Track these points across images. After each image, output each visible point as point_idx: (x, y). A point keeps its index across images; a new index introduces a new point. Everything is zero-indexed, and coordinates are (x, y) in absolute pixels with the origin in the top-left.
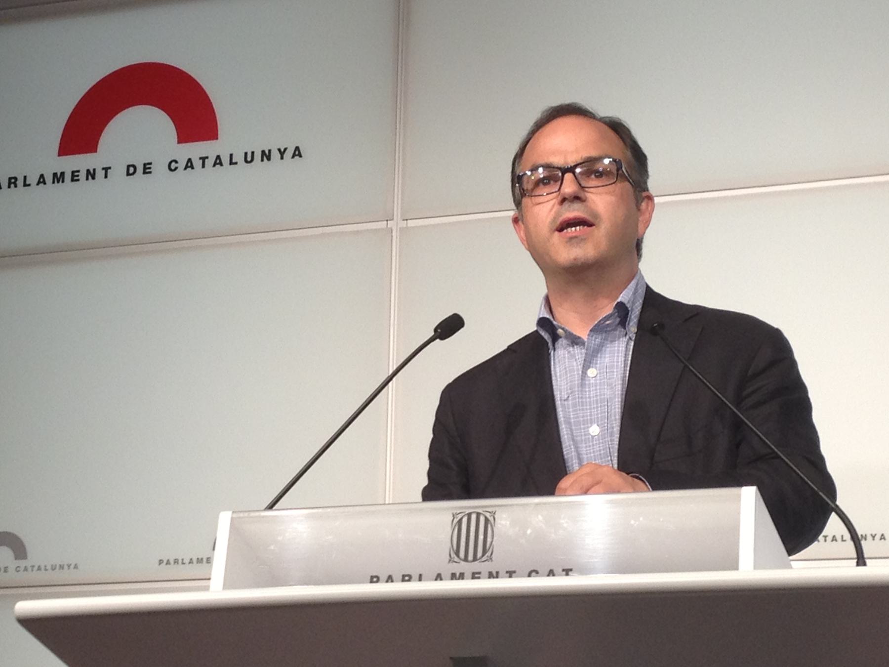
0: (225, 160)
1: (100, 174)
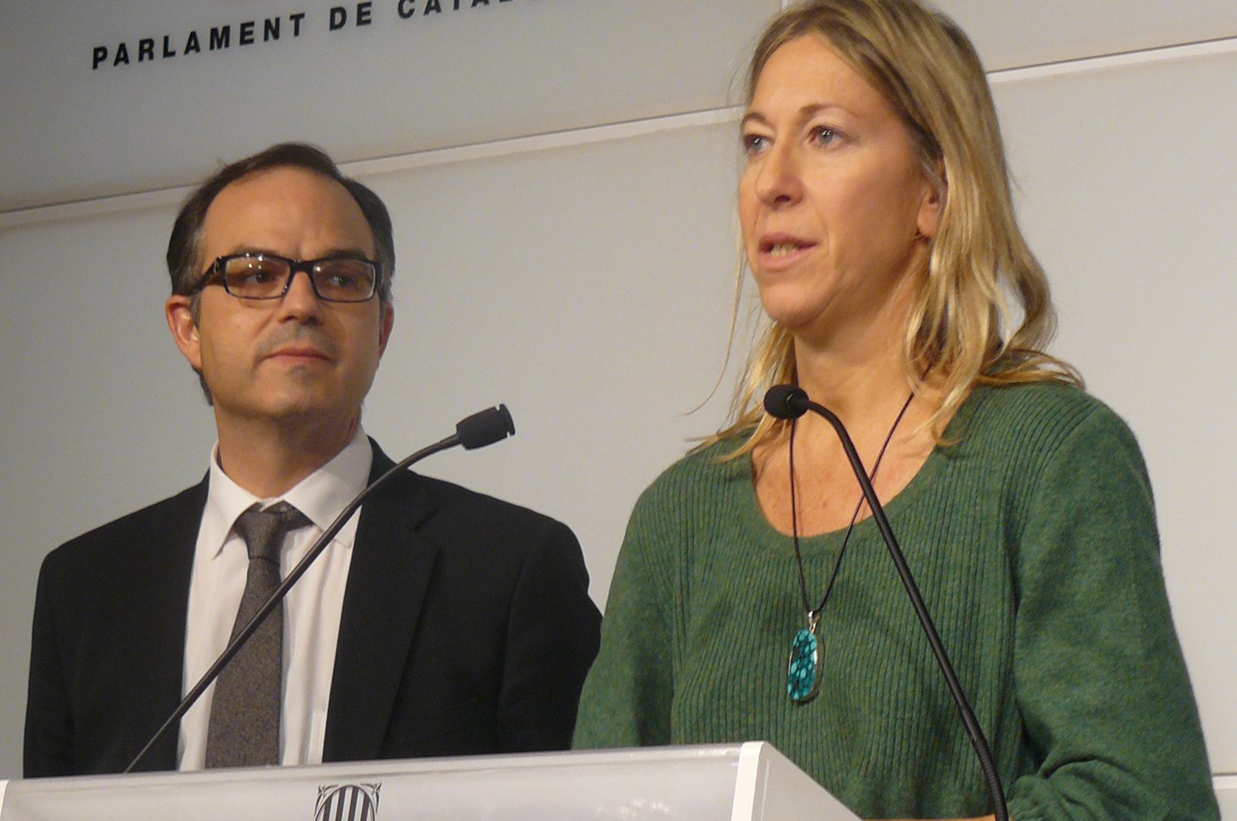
1: (287, 27)
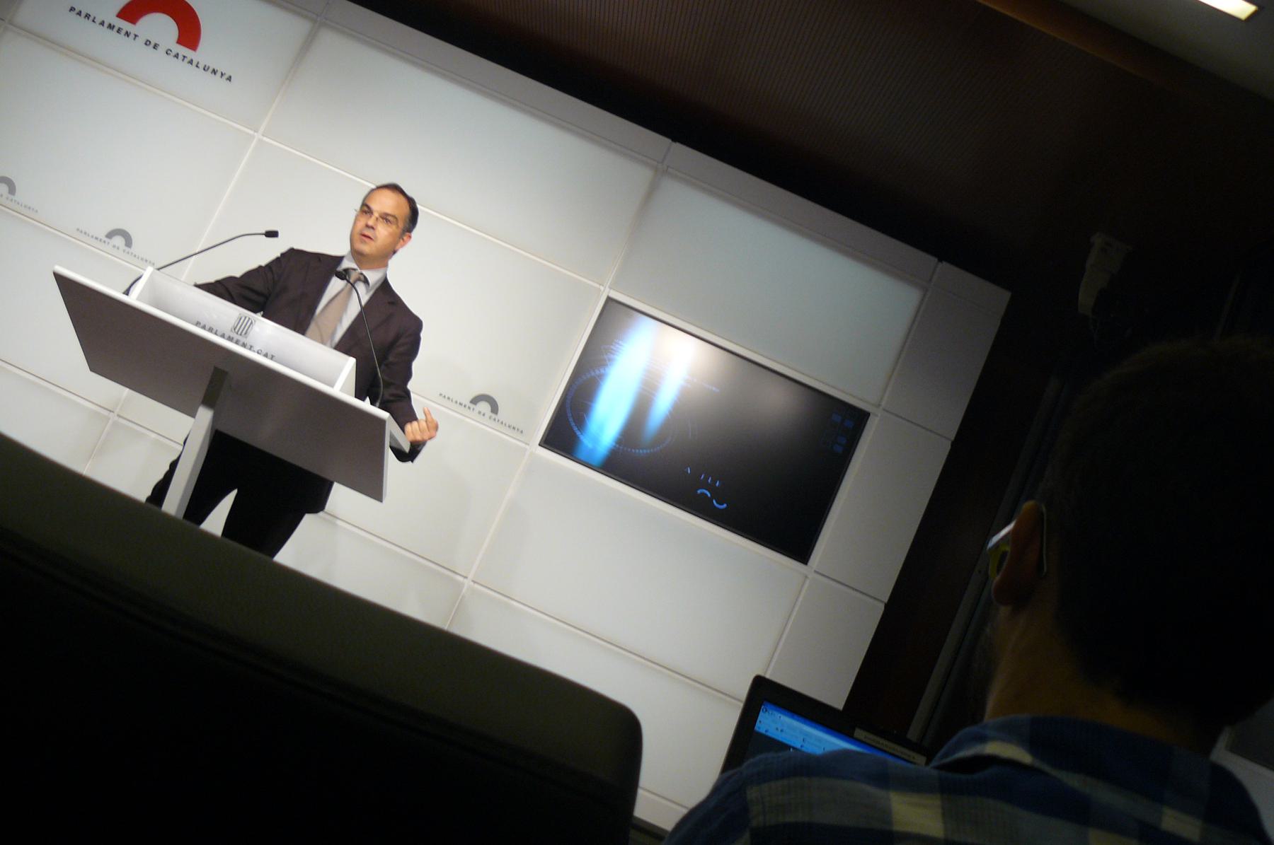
1: (132, 36)
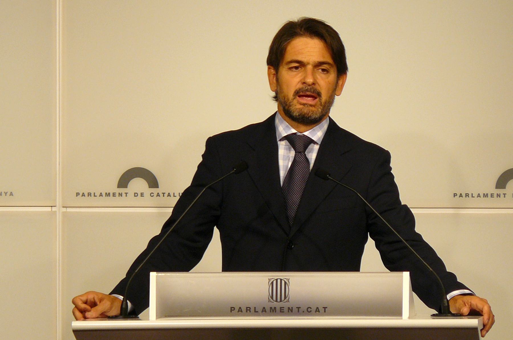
0: (172, 195)
